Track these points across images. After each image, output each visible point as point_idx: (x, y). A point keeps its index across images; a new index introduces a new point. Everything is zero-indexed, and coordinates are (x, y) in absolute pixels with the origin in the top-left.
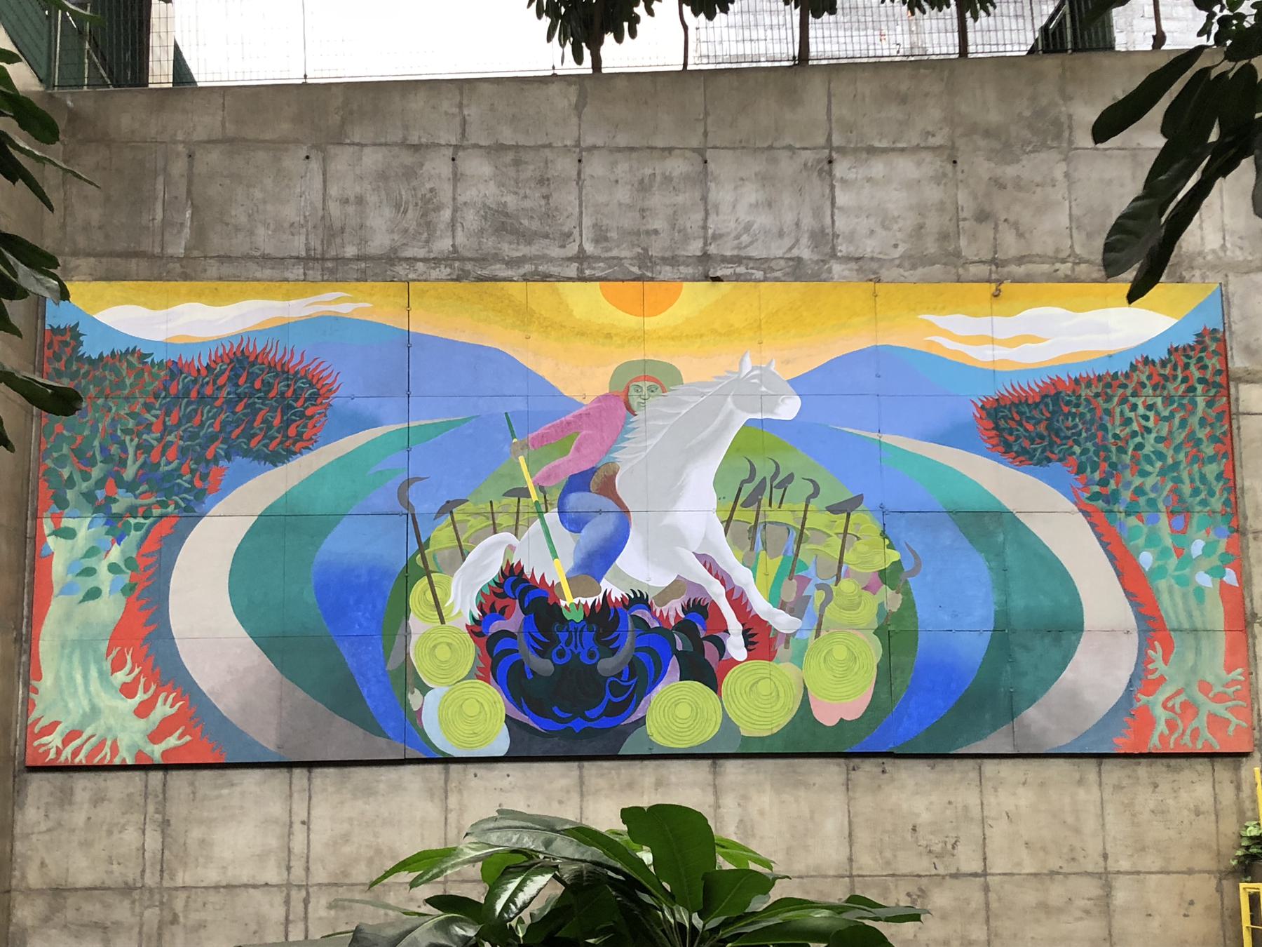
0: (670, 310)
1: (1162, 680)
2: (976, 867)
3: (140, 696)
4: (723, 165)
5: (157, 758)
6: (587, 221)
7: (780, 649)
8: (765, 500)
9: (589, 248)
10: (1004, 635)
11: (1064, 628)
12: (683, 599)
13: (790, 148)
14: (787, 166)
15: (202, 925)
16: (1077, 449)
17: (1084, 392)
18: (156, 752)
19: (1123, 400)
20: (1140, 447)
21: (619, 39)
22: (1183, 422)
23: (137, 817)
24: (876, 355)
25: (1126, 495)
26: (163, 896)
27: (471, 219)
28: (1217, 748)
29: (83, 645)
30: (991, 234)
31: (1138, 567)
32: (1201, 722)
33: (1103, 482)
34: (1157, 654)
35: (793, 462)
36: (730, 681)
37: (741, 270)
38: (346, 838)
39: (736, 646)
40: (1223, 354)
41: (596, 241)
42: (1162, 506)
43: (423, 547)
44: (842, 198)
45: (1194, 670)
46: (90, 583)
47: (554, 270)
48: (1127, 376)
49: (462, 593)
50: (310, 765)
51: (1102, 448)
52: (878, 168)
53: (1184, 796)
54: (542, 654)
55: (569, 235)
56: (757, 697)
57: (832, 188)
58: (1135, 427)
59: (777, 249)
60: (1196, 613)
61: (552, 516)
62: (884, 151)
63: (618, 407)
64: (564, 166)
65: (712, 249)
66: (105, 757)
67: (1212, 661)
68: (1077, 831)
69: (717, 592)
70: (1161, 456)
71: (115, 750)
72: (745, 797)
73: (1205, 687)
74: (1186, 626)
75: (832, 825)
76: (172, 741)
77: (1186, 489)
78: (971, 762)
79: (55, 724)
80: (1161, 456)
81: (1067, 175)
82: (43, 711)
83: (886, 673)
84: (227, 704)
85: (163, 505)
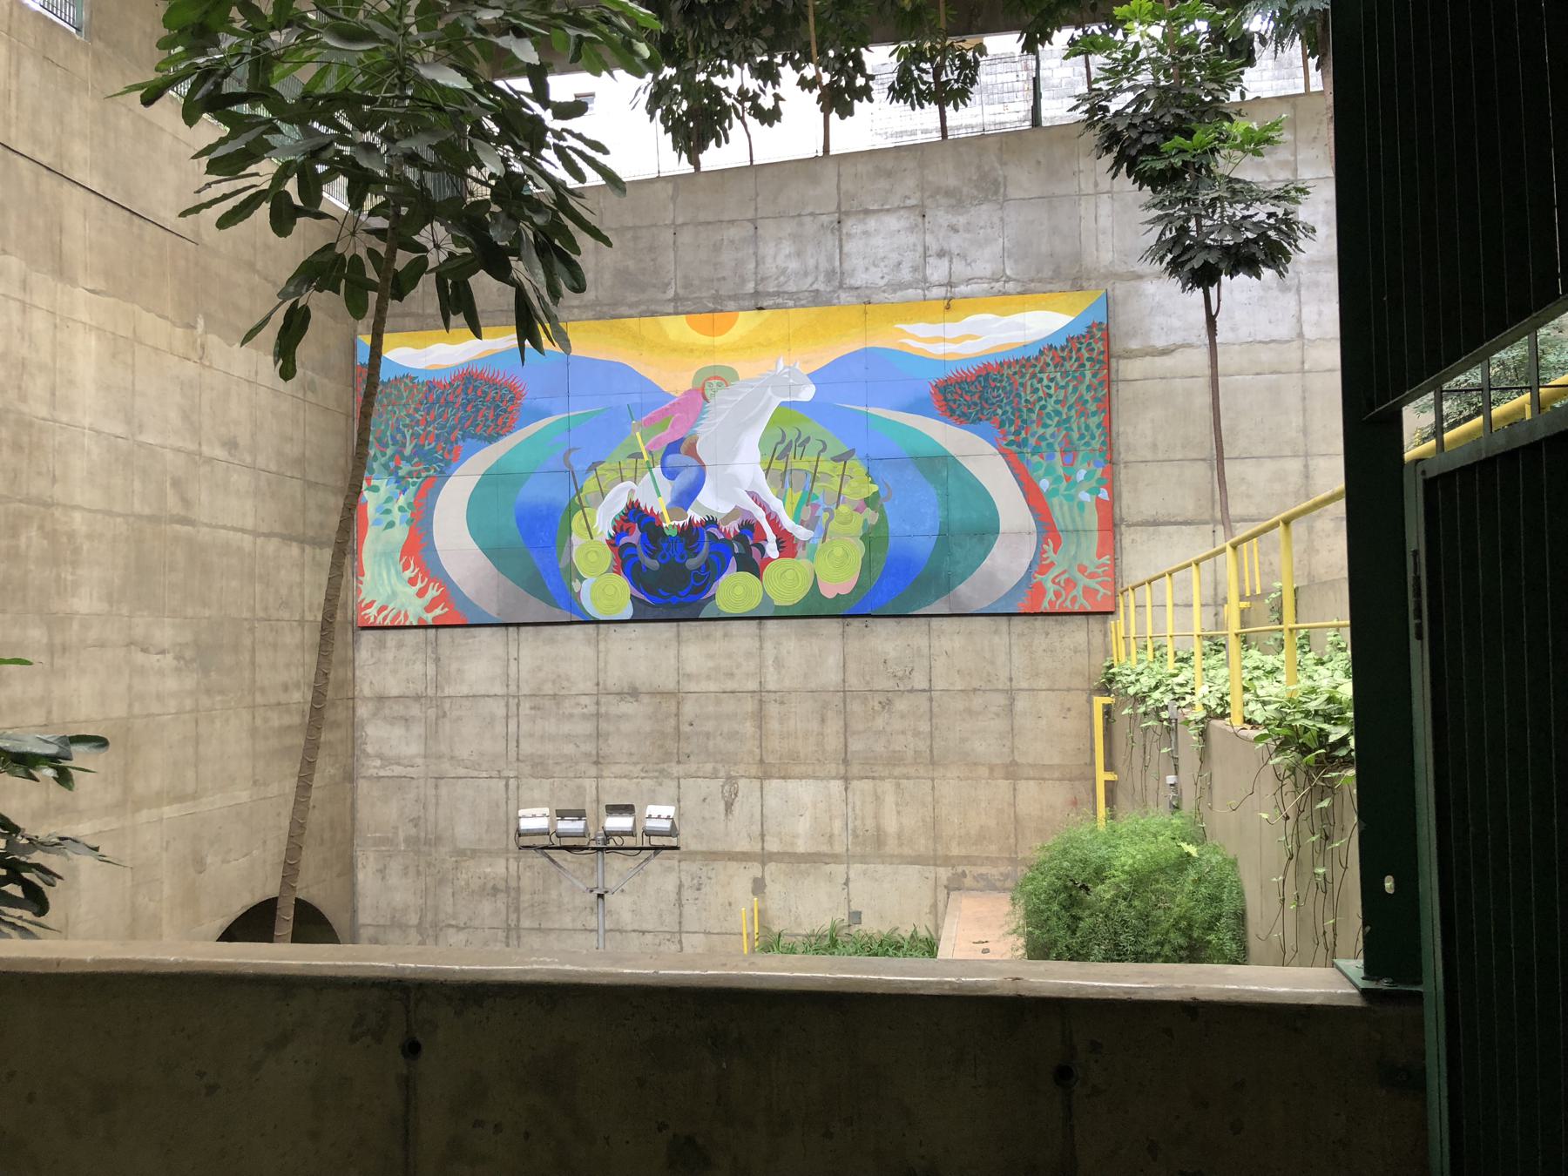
0: (731, 331)
1: (1052, 564)
2: (925, 685)
3: (419, 585)
4: (768, 229)
5: (430, 622)
6: (679, 275)
7: (800, 550)
8: (791, 454)
9: (681, 292)
10: (945, 537)
11: (986, 531)
12: (739, 521)
13: (812, 214)
14: (810, 226)
15: (459, 718)
16: (1000, 411)
17: (1006, 371)
18: (429, 618)
19: (1033, 375)
20: (1044, 407)
21: (718, 145)
22: (1075, 388)
23: (421, 656)
24: (866, 355)
25: (1032, 441)
26: (437, 701)
27: (607, 277)
28: (1089, 609)
29: (386, 554)
30: (947, 264)
31: (1038, 489)
32: (1078, 592)
33: (1017, 433)
34: (1049, 548)
35: (812, 428)
36: (767, 572)
37: (780, 301)
38: (540, 669)
39: (772, 549)
40: (1107, 338)
41: (685, 287)
42: (1057, 447)
43: (578, 491)
44: (846, 249)
45: (1075, 557)
46: (388, 518)
47: (658, 308)
48: (1037, 359)
49: (603, 519)
50: (518, 625)
51: (1017, 410)
52: (872, 223)
53: (1067, 640)
54: (651, 557)
55: (668, 284)
56: (784, 582)
57: (841, 240)
58: (1041, 394)
59: (806, 284)
60: (1078, 519)
61: (657, 470)
62: (874, 212)
63: (697, 398)
64: (667, 236)
65: (760, 288)
66: (401, 621)
67: (1088, 550)
68: (992, 663)
69: (760, 515)
70: (1058, 413)
71: (406, 616)
72: (779, 644)
73: (1082, 569)
74: (1070, 528)
75: (833, 660)
76: (438, 612)
77: (1075, 435)
78: (923, 620)
79: (372, 603)
80: (1058, 413)
81: (1002, 219)
82: (367, 594)
83: (867, 564)
84: (468, 589)
85: (427, 470)
